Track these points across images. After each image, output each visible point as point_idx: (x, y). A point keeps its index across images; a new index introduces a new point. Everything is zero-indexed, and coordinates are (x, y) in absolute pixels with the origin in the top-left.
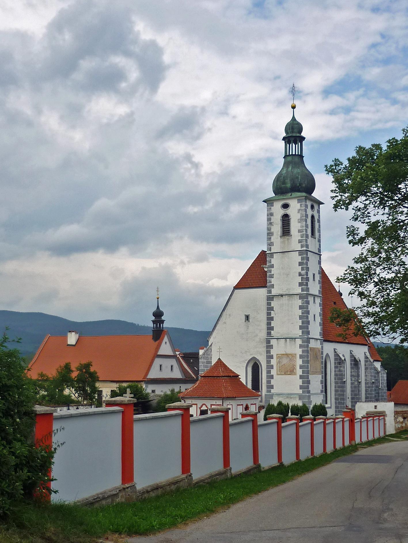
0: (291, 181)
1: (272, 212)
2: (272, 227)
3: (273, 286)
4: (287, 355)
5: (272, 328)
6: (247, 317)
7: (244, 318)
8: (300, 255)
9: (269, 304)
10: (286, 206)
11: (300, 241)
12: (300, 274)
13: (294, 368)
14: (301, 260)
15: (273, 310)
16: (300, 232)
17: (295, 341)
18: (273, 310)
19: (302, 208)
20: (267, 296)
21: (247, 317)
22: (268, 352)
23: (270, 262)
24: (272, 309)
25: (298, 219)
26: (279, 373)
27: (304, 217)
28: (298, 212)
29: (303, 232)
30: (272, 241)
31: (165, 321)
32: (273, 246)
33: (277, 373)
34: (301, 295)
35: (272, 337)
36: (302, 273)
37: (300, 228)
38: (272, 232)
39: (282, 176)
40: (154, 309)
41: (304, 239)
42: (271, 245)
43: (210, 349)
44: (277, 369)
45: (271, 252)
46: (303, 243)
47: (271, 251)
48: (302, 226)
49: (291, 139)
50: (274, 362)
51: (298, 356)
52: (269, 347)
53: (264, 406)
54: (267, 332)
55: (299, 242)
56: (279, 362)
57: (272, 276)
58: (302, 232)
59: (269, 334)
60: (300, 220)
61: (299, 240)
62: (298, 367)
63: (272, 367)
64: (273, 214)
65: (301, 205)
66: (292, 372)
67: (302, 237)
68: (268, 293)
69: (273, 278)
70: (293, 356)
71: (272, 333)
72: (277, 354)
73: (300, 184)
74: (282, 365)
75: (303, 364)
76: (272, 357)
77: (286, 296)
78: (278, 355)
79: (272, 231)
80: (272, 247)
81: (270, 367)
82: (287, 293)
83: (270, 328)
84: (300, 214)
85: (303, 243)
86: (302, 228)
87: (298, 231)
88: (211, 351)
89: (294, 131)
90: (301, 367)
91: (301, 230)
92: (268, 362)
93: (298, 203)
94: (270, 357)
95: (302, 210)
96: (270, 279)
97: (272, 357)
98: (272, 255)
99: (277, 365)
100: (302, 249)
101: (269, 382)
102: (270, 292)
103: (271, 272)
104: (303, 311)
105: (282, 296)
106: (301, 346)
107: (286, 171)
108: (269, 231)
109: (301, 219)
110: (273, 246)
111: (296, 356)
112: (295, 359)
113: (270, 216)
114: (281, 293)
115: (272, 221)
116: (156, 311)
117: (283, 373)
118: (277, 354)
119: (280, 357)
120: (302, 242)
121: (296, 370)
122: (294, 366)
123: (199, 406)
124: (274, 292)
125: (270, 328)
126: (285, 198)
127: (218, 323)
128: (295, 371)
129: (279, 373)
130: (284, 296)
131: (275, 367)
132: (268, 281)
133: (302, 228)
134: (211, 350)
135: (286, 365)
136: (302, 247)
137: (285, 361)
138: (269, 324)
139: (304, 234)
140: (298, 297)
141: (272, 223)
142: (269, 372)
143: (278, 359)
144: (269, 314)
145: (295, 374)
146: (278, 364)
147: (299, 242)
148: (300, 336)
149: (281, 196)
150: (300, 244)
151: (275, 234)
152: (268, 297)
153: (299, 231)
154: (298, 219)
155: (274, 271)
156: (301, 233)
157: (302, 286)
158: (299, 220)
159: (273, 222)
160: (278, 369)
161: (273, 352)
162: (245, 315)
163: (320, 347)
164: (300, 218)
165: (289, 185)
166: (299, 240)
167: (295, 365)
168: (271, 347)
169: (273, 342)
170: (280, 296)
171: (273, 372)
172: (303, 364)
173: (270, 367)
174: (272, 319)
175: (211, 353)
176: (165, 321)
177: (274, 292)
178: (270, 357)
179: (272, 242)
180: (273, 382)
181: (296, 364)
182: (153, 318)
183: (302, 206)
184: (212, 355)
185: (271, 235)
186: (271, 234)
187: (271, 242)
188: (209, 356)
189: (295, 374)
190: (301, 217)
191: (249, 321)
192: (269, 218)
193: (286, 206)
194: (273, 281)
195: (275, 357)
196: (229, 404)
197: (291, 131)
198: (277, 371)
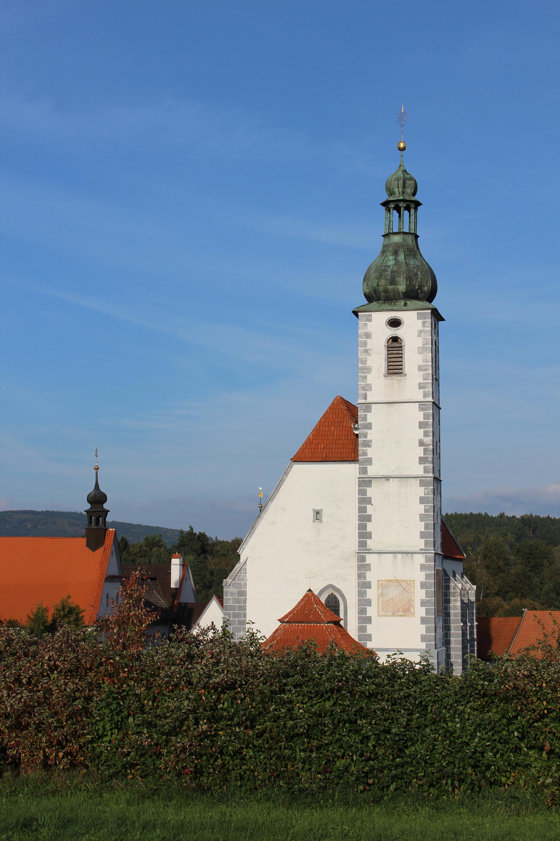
0: (407, 280)
1: (368, 331)
2: (369, 358)
3: (369, 461)
4: (398, 582)
6: (318, 514)
7: (311, 515)
8: (421, 409)
9: (362, 492)
10: (395, 323)
11: (421, 386)
12: (421, 443)
13: (411, 604)
14: (424, 419)
15: (370, 503)
16: (422, 370)
17: (412, 559)
18: (370, 503)
19: (426, 328)
20: (359, 478)
21: (318, 514)
22: (361, 576)
23: (365, 418)
24: (369, 501)
25: (419, 348)
26: (382, 613)
27: (429, 344)
28: (419, 335)
29: (427, 370)
30: (368, 383)
31: (109, 511)
32: (371, 390)
33: (378, 613)
34: (424, 479)
35: (369, 550)
36: (425, 441)
37: (421, 363)
38: (369, 366)
39: (389, 269)
40: (91, 488)
41: (428, 383)
42: (366, 388)
43: (243, 570)
44: (378, 607)
45: (366, 402)
46: (427, 390)
47: (365, 398)
48: (426, 359)
49: (401, 205)
50: (371, 594)
51: (418, 585)
54: (359, 542)
55: (420, 388)
56: (382, 594)
57: (368, 444)
58: (425, 371)
59: (362, 544)
60: (421, 350)
61: (420, 384)
62: (417, 604)
63: (369, 602)
64: (370, 334)
65: (424, 323)
66: (407, 611)
67: (425, 379)
68: (360, 473)
69: (370, 446)
70: (410, 583)
71: (368, 544)
72: (378, 581)
73: (420, 287)
74: (389, 600)
75: (427, 599)
76: (368, 585)
77: (396, 479)
79: (368, 364)
80: (368, 393)
82: (397, 473)
84: (423, 339)
85: (427, 390)
86: (426, 364)
87: (418, 368)
88: (246, 573)
89: (406, 190)
90: (423, 603)
91: (424, 366)
92: (362, 594)
93: (418, 319)
94: (364, 585)
95: (425, 332)
96: (364, 448)
97: (368, 585)
98: (368, 406)
99: (378, 600)
100: (426, 400)
102: (364, 471)
103: (366, 437)
104: (427, 507)
105: (387, 478)
106: (423, 567)
107: (394, 261)
108: (363, 364)
109: (423, 347)
110: (371, 390)
111: (414, 583)
112: (412, 590)
113: (364, 337)
114: (386, 473)
115: (368, 348)
116: (95, 494)
117: (390, 614)
118: (378, 581)
119: (384, 585)
120: (425, 388)
121: (413, 607)
124: (372, 471)
126: (395, 308)
127: (259, 524)
128: (412, 610)
129: (382, 613)
130: (391, 479)
131: (374, 603)
132: (360, 452)
133: (426, 364)
134: (246, 570)
136: (425, 395)
137: (393, 592)
138: (362, 527)
139: (428, 374)
140: (418, 482)
141: (369, 351)
142: (362, 611)
143: (380, 590)
144: (362, 510)
145: (413, 615)
146: (381, 598)
147: (420, 388)
148: (421, 549)
149: (386, 305)
150: (422, 391)
151: (374, 370)
152: (361, 480)
153: (420, 368)
154: (419, 348)
155: (371, 435)
156: (425, 372)
157: (425, 464)
158: (420, 350)
159: (370, 349)
160: (381, 606)
161: (370, 576)
162: (314, 510)
164: (422, 346)
165: (402, 288)
166: (420, 384)
167: (412, 600)
168: (368, 567)
169: (370, 559)
170: (383, 480)
171: (371, 611)
172: (427, 599)
174: (369, 518)
175: (245, 576)
176: (109, 511)
177: (372, 471)
178: (364, 585)
179: (368, 385)
181: (414, 598)
182: (88, 506)
183: (427, 324)
184: (246, 580)
185: (366, 371)
186: (367, 369)
187: (365, 384)
188: (242, 582)
189: (413, 615)
190: (423, 345)
191: (321, 521)
192: (364, 341)
193: (395, 323)
194: (371, 452)
195: (374, 585)
197: (400, 189)
198: (378, 610)
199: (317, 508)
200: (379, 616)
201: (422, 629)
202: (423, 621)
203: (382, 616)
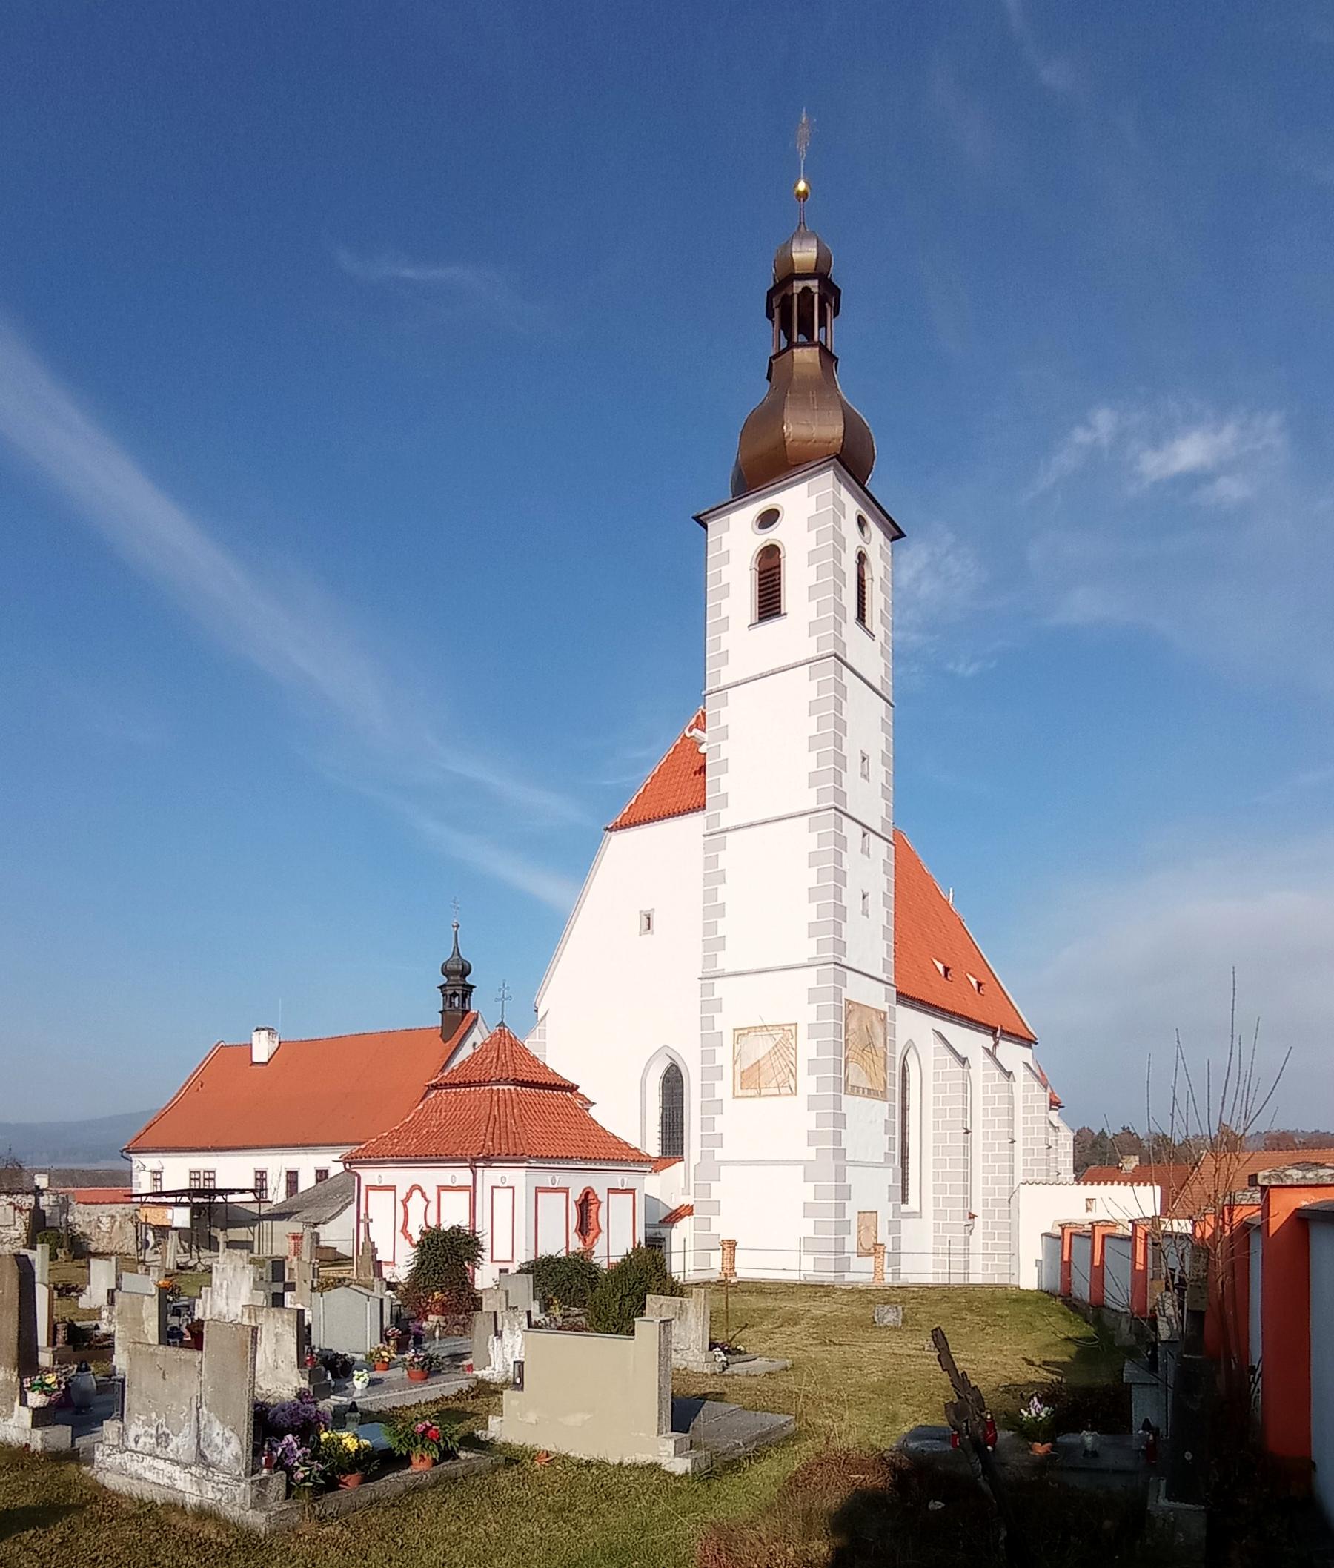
5: (721, 943)
7: (636, 923)
22: (707, 1022)
26: (739, 1092)
33: (734, 1094)
52: (711, 1006)
53: (693, 1206)
59: (710, 959)
78: (737, 1033)
81: (713, 1072)
83: (713, 943)
92: (708, 1056)
101: (707, 1123)
112: (793, 1042)
121: (794, 1077)
122: (790, 1065)
123: (401, 1194)
125: (713, 943)
135: (762, 1062)
137: (760, 1048)
142: (707, 1090)
145: (793, 1093)
163: (884, 1007)
173: (713, 1072)
178: (710, 1039)
180: (721, 1124)
189: (793, 1093)
191: (653, 933)
196: (501, 1185)
199: (646, 908)
200: (735, 1097)
201: (810, 1121)
202: (812, 1102)
203: (738, 1097)
